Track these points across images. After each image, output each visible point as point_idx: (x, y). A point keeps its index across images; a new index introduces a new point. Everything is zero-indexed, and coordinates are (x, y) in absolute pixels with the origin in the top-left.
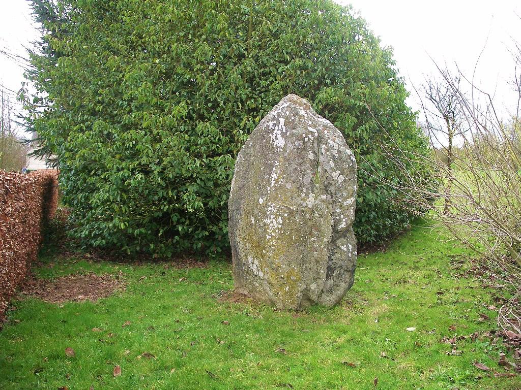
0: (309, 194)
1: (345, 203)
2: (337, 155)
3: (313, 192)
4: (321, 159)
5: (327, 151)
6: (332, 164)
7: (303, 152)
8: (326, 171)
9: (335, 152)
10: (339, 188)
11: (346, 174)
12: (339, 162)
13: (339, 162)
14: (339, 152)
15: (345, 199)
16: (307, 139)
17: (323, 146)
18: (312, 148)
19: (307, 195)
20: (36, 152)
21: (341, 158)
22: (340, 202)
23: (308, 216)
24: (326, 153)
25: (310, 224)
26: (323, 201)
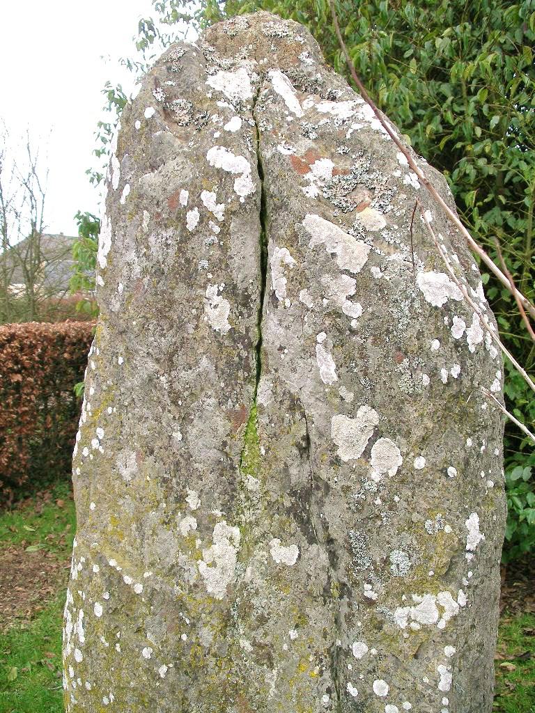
0: (214, 520)
1: (400, 616)
2: (355, 310)
3: (230, 515)
4: (273, 331)
5: (298, 280)
6: (327, 367)
7: (181, 292)
8: (295, 405)
9: (341, 290)
10: (366, 517)
11: (418, 433)
12: (375, 355)
13: (375, 355)
14: (366, 286)
15: (403, 592)
16: (193, 218)
17: (279, 254)
18: (221, 265)
19: (205, 528)
20: (22, 321)
21: (380, 331)
22: (370, 603)
23: (207, 635)
24: (292, 293)
25: (215, 680)
26: (276, 575)
